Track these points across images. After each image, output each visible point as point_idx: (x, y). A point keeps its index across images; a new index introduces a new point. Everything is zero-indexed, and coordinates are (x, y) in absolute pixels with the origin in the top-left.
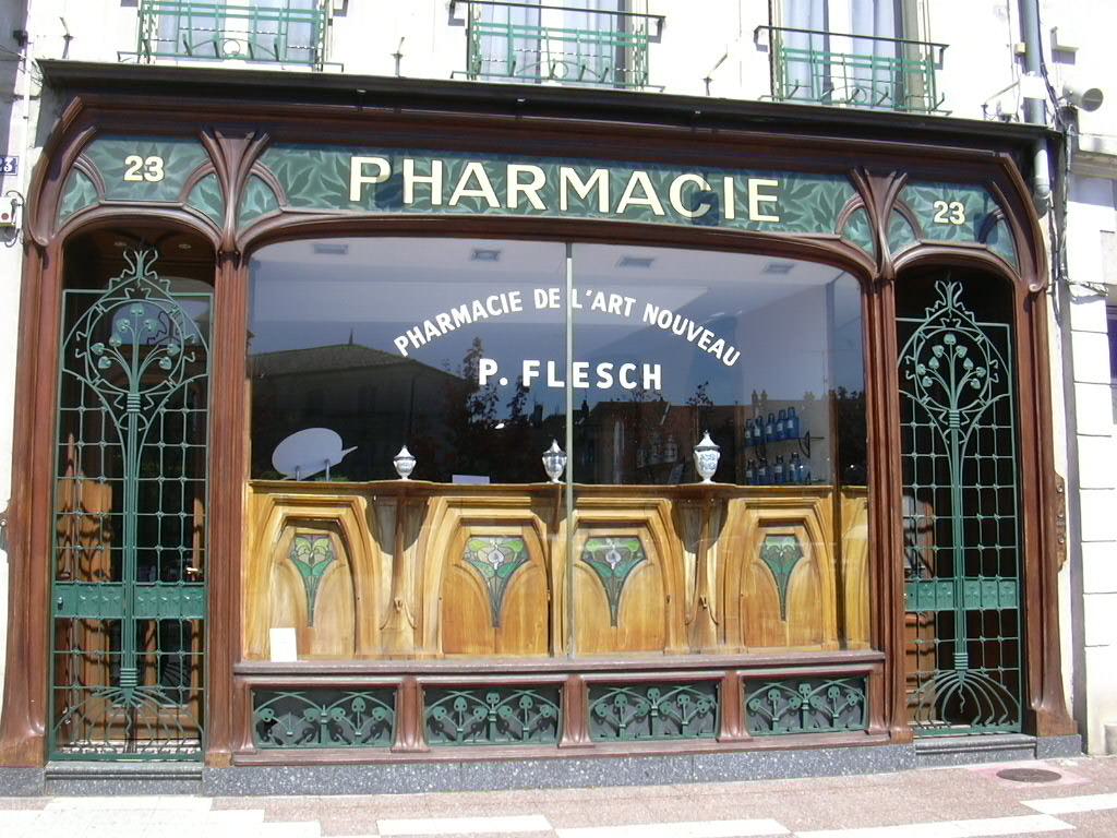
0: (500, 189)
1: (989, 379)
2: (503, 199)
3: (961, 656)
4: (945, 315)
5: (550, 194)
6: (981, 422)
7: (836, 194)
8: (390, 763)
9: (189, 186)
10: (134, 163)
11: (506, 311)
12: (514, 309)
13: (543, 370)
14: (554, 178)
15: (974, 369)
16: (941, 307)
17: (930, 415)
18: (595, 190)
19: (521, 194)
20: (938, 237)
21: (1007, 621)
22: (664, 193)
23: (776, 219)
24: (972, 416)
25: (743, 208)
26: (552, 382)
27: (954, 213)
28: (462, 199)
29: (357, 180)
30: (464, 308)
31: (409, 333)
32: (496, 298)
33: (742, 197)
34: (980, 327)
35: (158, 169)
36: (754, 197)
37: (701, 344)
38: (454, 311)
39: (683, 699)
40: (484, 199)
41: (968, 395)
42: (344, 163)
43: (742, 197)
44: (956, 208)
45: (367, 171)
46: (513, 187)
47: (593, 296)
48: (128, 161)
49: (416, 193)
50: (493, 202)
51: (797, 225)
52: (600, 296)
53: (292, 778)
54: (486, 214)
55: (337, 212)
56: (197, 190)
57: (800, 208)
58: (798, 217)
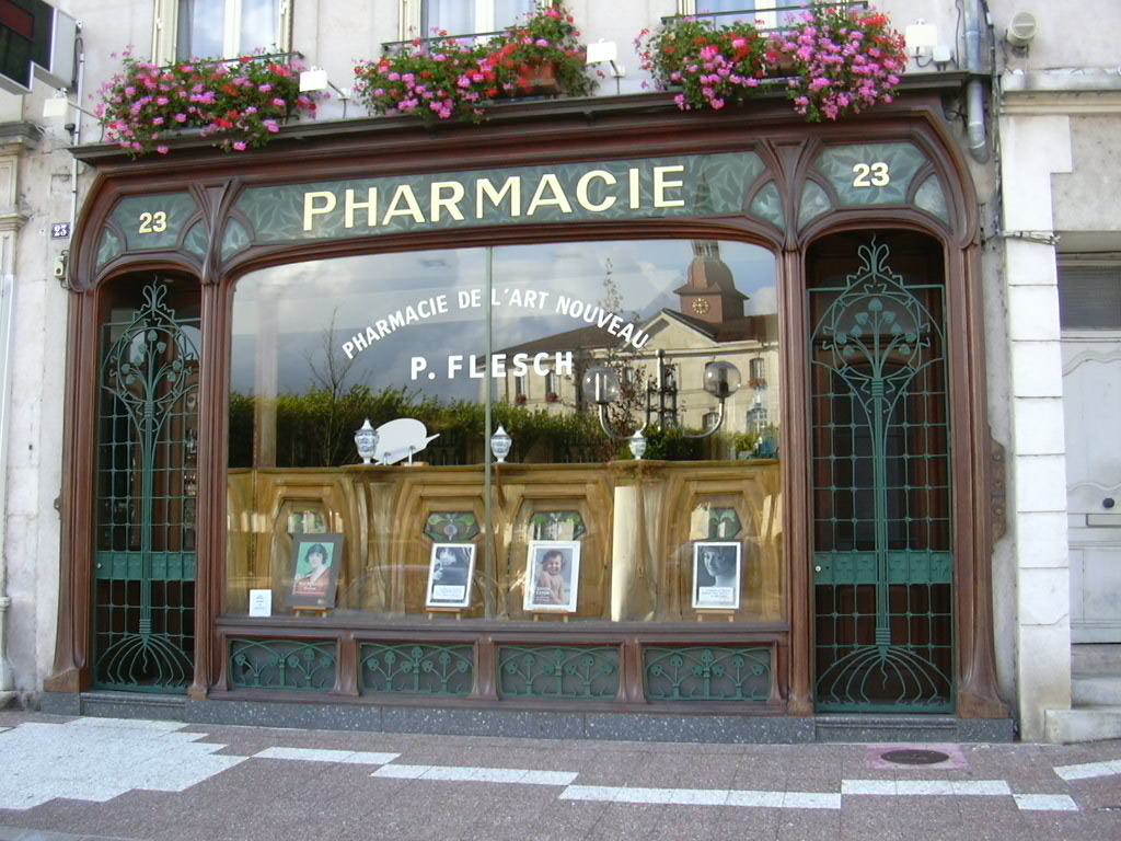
1: (919, 344)
2: (427, 214)
3: (883, 633)
4: (870, 280)
5: (467, 205)
6: (909, 389)
8: (325, 704)
9: (186, 230)
11: (434, 313)
12: (441, 311)
13: (465, 363)
14: (471, 191)
17: (850, 384)
18: (508, 198)
19: (443, 208)
21: (942, 595)
22: (570, 191)
23: (682, 203)
24: (899, 384)
25: (649, 196)
26: (473, 374)
27: (876, 174)
28: (394, 218)
29: (309, 211)
30: (399, 314)
31: (354, 339)
32: (425, 302)
33: (647, 186)
35: (162, 221)
36: (659, 185)
37: (610, 330)
38: (391, 317)
41: (892, 366)
43: (647, 186)
44: (880, 169)
46: (436, 202)
47: (511, 292)
48: (142, 218)
50: (419, 218)
52: (517, 292)
53: (251, 712)
54: (414, 228)
56: (191, 236)
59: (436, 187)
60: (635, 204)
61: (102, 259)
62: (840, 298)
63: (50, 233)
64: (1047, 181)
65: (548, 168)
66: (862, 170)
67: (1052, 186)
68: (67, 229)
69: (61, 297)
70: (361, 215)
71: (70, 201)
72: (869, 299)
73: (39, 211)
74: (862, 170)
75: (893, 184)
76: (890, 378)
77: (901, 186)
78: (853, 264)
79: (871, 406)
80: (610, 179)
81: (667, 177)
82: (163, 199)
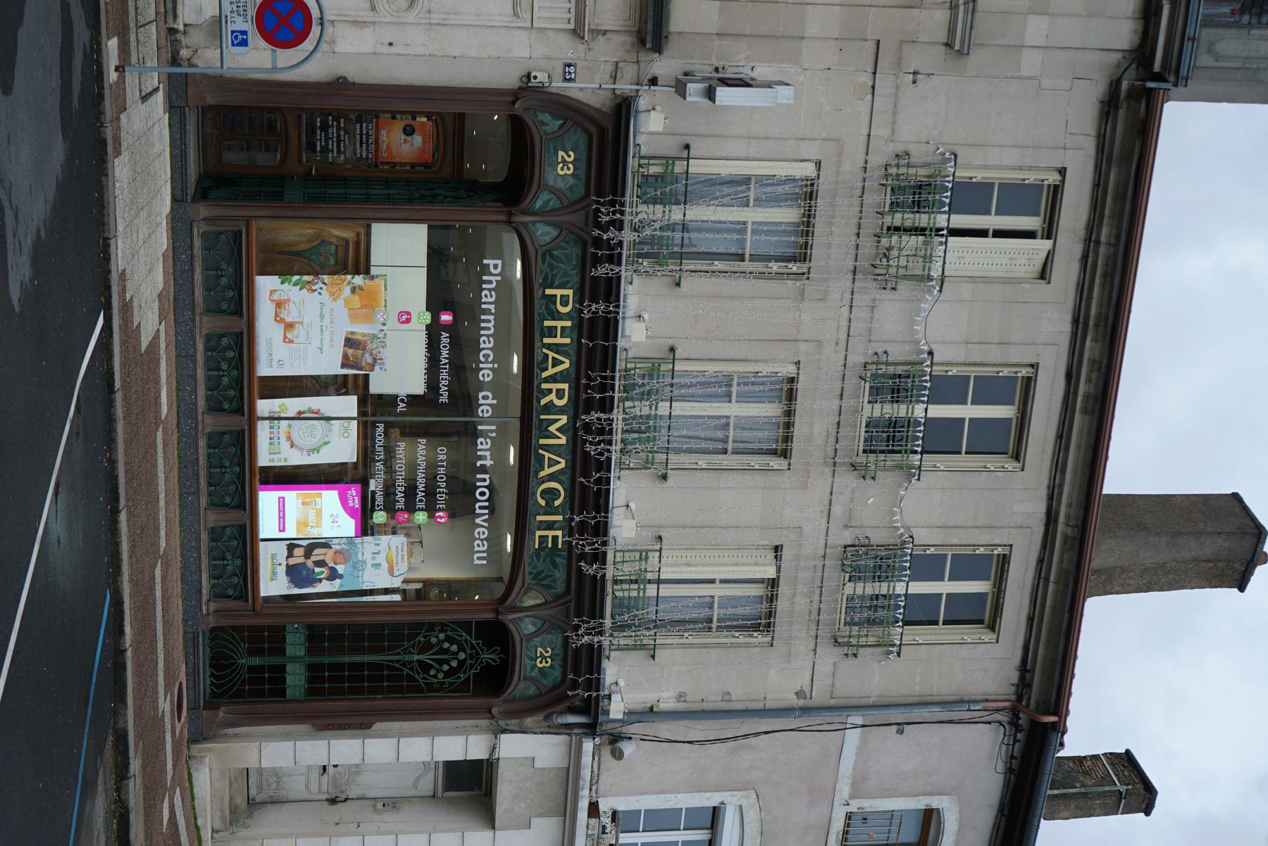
0: (553, 379)
1: (435, 680)
2: (546, 380)
4: (477, 653)
5: (549, 408)
6: (408, 674)
7: (553, 585)
9: (553, 190)
10: (569, 156)
14: (561, 411)
15: (442, 671)
16: (482, 650)
19: (550, 391)
20: (528, 649)
21: (279, 690)
22: (552, 477)
23: (537, 547)
24: (412, 669)
25: (543, 526)
29: (559, 292)
34: (469, 676)
35: (566, 171)
36: (550, 533)
39: (232, 488)
40: (547, 369)
41: (425, 667)
42: (569, 285)
43: (550, 526)
44: (547, 662)
45: (563, 299)
46: (554, 386)
48: (571, 153)
49: (550, 328)
50: (544, 375)
51: (533, 560)
53: (184, 256)
54: (536, 370)
55: (539, 280)
56: (552, 196)
57: (544, 562)
58: (538, 561)
59: (565, 386)
60: (539, 518)
61: (541, 117)
62: (467, 637)
63: (568, 61)
64: (530, 755)
65: (570, 464)
66: (547, 652)
67: (526, 758)
68: (570, 80)
70: (551, 332)
71: (593, 83)
72: (466, 653)
73: (590, 49)
75: (536, 670)
76: (415, 664)
77: (535, 673)
78: (489, 646)
79: (398, 654)
80: (557, 503)
81: (555, 538)
82: (582, 173)
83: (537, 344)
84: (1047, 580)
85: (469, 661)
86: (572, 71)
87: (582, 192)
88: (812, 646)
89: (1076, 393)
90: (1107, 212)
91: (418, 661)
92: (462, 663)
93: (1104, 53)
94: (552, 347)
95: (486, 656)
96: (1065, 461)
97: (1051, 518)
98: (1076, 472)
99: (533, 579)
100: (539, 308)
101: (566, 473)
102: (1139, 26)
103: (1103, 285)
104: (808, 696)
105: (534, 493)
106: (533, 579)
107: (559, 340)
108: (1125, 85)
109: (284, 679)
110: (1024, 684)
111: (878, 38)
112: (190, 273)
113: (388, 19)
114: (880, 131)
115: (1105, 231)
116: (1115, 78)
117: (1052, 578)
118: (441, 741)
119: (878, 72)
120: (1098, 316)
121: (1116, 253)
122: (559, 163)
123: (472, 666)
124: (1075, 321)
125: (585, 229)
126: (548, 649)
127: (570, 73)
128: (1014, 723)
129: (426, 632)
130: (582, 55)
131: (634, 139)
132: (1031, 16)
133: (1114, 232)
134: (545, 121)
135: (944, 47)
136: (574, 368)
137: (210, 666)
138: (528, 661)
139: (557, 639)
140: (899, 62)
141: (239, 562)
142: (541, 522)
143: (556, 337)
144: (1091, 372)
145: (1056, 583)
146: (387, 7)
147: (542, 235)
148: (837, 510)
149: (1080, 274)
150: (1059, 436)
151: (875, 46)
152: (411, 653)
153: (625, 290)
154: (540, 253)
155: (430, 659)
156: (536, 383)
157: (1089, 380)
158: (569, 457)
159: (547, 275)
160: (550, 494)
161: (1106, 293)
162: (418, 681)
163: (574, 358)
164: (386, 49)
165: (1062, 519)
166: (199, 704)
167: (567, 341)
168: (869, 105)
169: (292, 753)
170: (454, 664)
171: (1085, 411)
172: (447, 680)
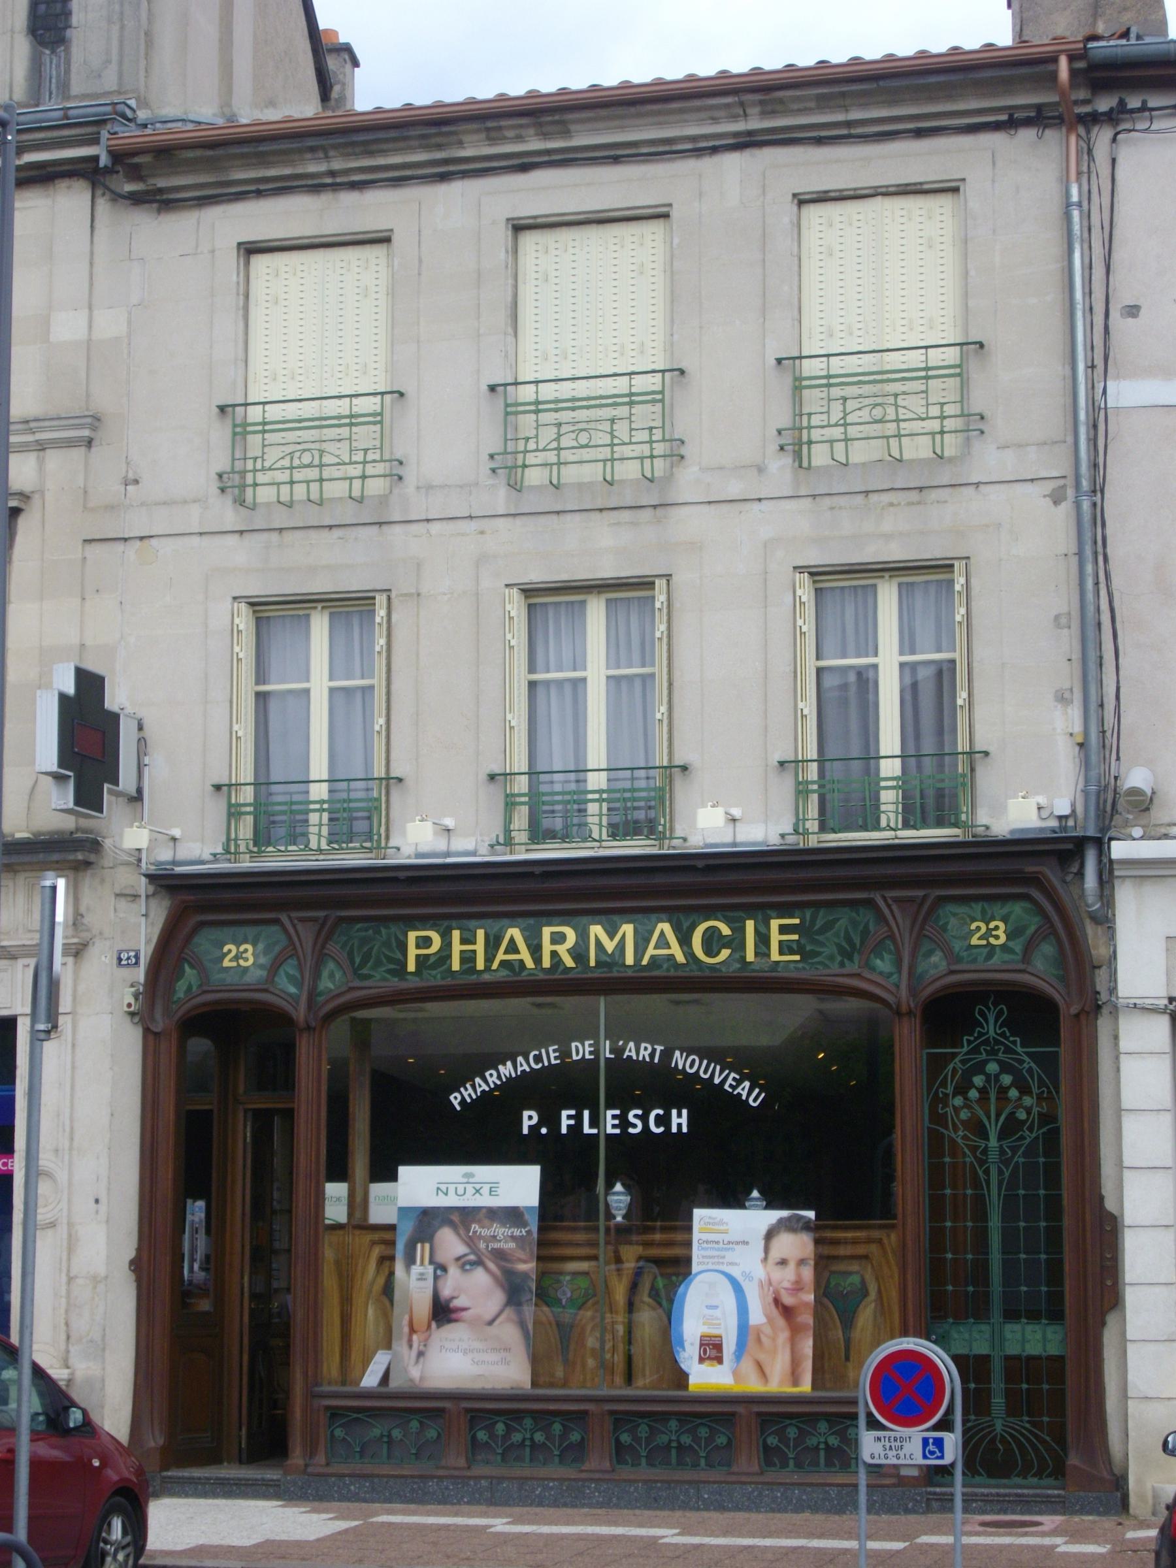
0: (536, 950)
2: (538, 960)
3: (998, 1401)
4: (986, 1042)
5: (579, 954)
7: (861, 928)
8: (432, 1477)
9: (274, 968)
11: (546, 1064)
12: (553, 1062)
13: (578, 1118)
14: (583, 936)
15: (1020, 1099)
16: (981, 1035)
17: (966, 1150)
18: (621, 946)
19: (554, 954)
20: (974, 960)
22: (685, 940)
23: (797, 958)
24: (1014, 1150)
25: (764, 949)
26: (587, 1130)
27: (994, 933)
28: (503, 963)
29: (412, 952)
30: (509, 1064)
31: (462, 1089)
32: (537, 1053)
33: (763, 939)
34: (1025, 1053)
35: (249, 955)
36: (775, 937)
37: (726, 1087)
38: (501, 1067)
39: (703, 1432)
40: (521, 961)
41: (1011, 1128)
42: (401, 938)
43: (763, 939)
44: (997, 928)
45: (421, 944)
46: (547, 947)
47: (626, 1044)
48: (226, 949)
49: (463, 960)
50: (530, 964)
51: (819, 963)
52: (631, 1045)
53: (352, 1488)
55: (395, 983)
56: (281, 972)
57: (822, 944)
58: (818, 954)
59: (547, 931)
60: (750, 956)
61: (180, 994)
62: (957, 1060)
63: (115, 961)
64: (1162, 944)
65: (663, 916)
66: (978, 928)
67: (1167, 950)
68: (137, 957)
69: (133, 1037)
70: (468, 958)
71: (140, 925)
72: (985, 1062)
73: (101, 933)
74: (978, 928)
75: (1011, 944)
76: (1005, 1143)
77: (1018, 946)
78: (970, 1024)
79: (987, 1172)
80: (726, 930)
81: (783, 929)
82: (251, 931)
83: (487, 977)
84: (849, 124)
85: (1001, 1056)
86: (126, 956)
87: (275, 928)
88: (971, 489)
89: (548, 152)
90: (287, 171)
91: (1000, 1139)
92: (1005, 1068)
93: (97, 224)
94: (491, 956)
95: (991, 1029)
96: (652, 142)
97: (746, 142)
98: (660, 124)
99: (851, 959)
100: (435, 979)
101: (678, 919)
102: (63, 184)
103: (383, 152)
104: (1061, 482)
105: (712, 967)
106: (851, 959)
107: (480, 947)
108: (129, 187)
109: (1030, 1358)
110: (1039, 118)
111: (81, 542)
112: (376, 1480)
113: (64, 1205)
114: (193, 519)
115: (312, 168)
116: (128, 202)
117: (840, 117)
118: (1130, 1095)
119: (122, 536)
120: (428, 148)
121: (335, 147)
122: (988, 942)
123: (1008, 1050)
124: (444, 178)
125: (320, 922)
126: (973, 926)
127: (128, 958)
128: (1112, 118)
129: (947, 1128)
130: (108, 943)
131: (203, 862)
132: (52, 338)
133: (309, 156)
134: (185, 988)
135: (93, 450)
136: (520, 920)
137: (1008, 1476)
138: (996, 961)
139: (954, 915)
140: (111, 508)
141: (823, 1426)
142: (756, 954)
143: (474, 952)
144: (505, 138)
145: (846, 109)
146: (50, 1207)
147: (334, 983)
148: (735, 489)
149: (381, 187)
150: (616, 160)
151: (93, 544)
152: (985, 1151)
153: (409, 857)
154: (357, 983)
155: (997, 1120)
156: (541, 976)
157: (519, 138)
158: (654, 917)
159: (389, 971)
160: (712, 942)
161: (390, 146)
162: (1037, 1138)
163: (505, 921)
164: (103, 1207)
165: (740, 126)
166: (1054, 1496)
167: (480, 934)
168: (164, 540)
169: (1152, 1347)
170: (1007, 1079)
171: (566, 133)
172: (1035, 1090)
